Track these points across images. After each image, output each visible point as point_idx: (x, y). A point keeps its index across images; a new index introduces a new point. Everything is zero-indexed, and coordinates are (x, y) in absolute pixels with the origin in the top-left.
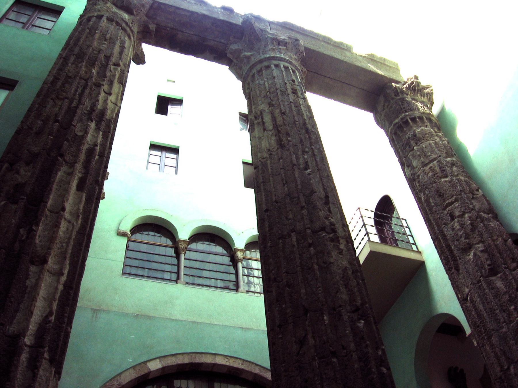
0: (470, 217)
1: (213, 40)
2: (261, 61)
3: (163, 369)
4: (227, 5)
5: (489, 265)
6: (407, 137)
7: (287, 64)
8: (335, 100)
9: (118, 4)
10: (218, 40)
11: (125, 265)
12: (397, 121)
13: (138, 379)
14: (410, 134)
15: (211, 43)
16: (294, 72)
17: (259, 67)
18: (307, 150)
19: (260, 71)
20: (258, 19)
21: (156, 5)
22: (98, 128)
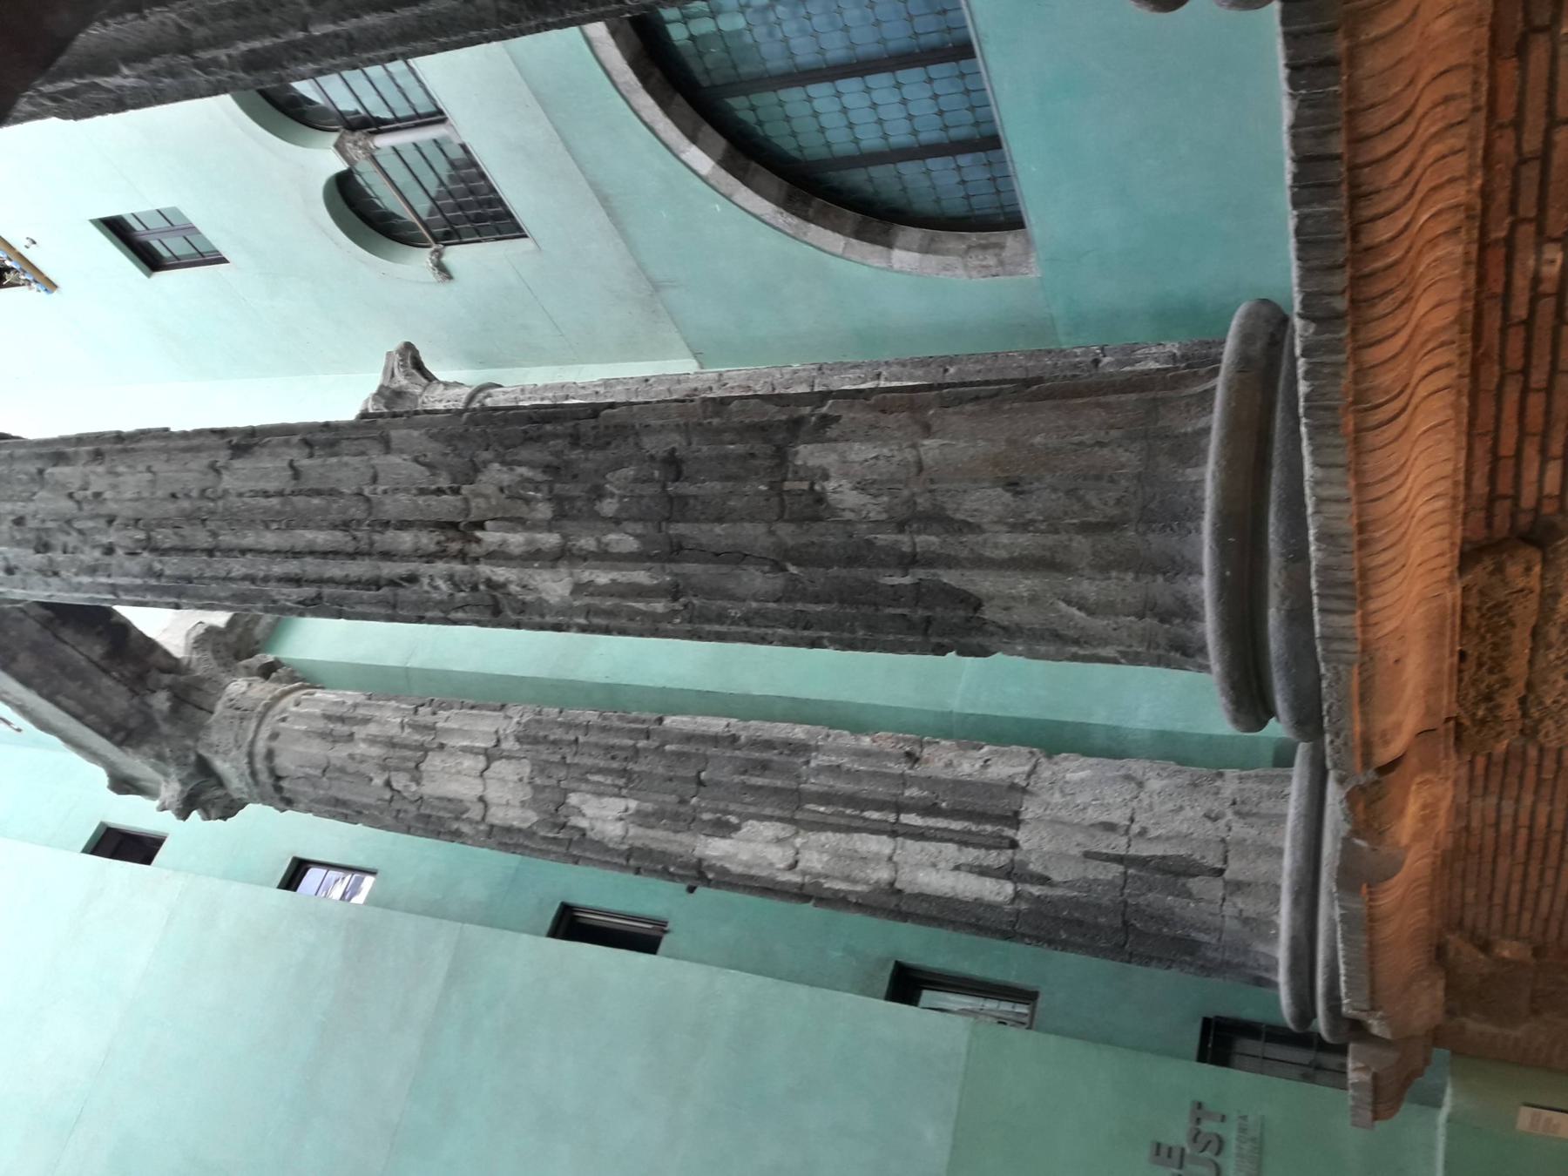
21: (120, 736)
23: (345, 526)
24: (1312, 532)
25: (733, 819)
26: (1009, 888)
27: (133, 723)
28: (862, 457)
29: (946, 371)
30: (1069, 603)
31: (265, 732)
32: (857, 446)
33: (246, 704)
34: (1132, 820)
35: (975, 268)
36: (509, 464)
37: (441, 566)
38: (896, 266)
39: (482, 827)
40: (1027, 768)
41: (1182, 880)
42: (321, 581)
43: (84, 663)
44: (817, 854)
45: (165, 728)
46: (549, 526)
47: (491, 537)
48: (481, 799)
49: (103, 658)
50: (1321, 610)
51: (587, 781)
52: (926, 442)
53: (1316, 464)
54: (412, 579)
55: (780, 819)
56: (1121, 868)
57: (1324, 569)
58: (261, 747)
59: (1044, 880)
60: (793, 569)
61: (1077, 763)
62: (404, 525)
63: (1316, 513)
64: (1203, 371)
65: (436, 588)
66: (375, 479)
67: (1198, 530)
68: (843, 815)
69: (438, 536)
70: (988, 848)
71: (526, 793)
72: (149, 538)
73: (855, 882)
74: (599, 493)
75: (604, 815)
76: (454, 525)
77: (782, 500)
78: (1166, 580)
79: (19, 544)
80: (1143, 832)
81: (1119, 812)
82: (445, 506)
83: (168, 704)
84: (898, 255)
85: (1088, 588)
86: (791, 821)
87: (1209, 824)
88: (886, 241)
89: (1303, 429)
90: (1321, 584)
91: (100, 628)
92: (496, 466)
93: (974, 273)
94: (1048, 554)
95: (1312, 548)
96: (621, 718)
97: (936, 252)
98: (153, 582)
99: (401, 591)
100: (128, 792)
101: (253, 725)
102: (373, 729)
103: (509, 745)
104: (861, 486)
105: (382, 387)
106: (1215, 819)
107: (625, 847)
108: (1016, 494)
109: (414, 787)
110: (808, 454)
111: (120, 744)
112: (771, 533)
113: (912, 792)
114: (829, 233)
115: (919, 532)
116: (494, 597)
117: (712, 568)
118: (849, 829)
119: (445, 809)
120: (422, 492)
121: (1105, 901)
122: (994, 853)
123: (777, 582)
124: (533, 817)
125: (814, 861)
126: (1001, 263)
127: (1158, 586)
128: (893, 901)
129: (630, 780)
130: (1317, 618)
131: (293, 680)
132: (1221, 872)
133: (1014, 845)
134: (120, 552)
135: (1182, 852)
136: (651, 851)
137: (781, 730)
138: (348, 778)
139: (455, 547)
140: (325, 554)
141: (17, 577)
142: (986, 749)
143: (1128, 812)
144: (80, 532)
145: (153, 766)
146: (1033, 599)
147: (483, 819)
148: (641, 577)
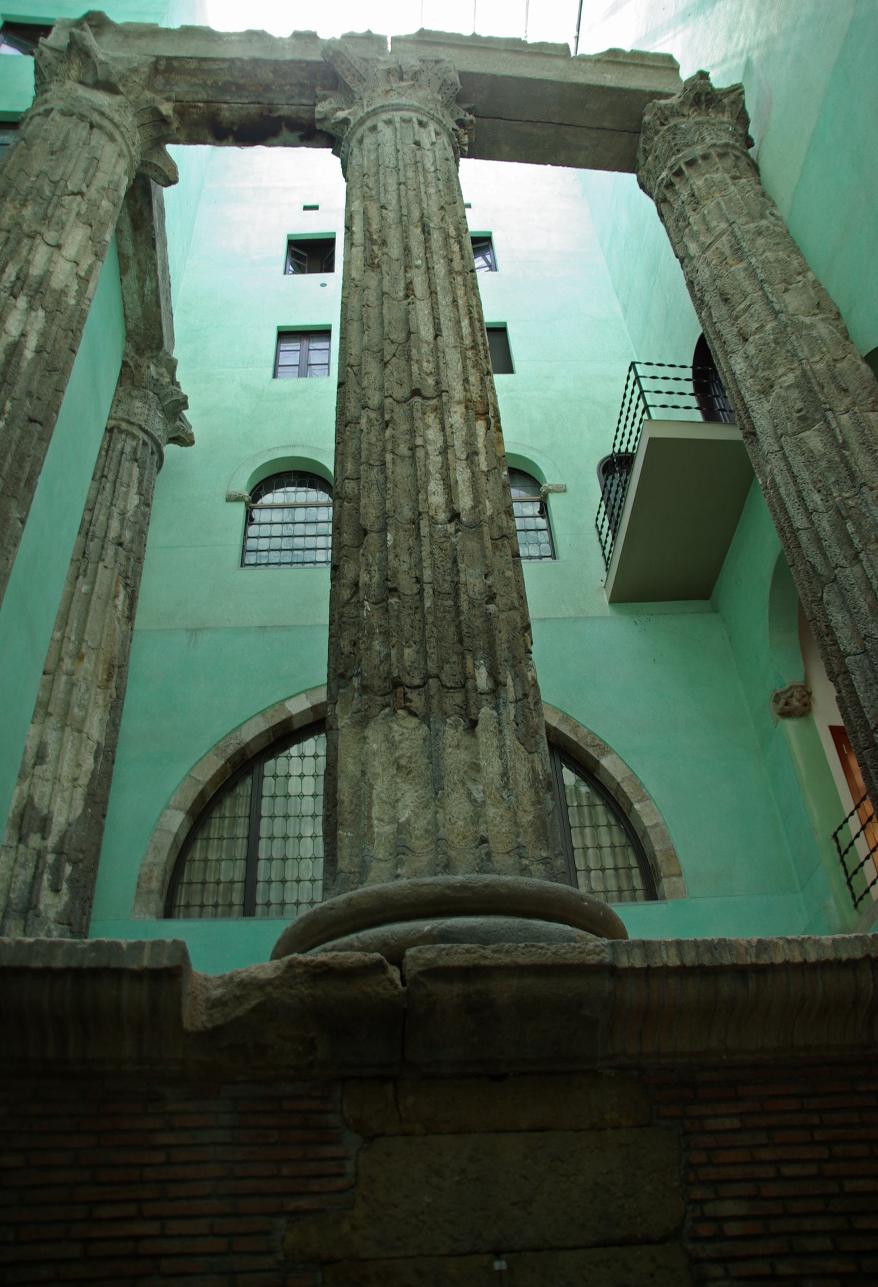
0: (773, 329)
1: (288, 104)
2: (361, 122)
4: (302, 28)
5: (800, 411)
6: (680, 203)
7: (406, 114)
8: (553, 164)
10: (295, 101)
11: (244, 551)
12: (664, 174)
13: (273, 729)
14: (685, 195)
15: (285, 111)
16: (421, 124)
17: (358, 135)
18: (419, 262)
19: (361, 141)
20: (369, 38)
21: (162, 65)
22: (31, 308)
27: (160, 80)
35: (151, 871)
38: (168, 812)
43: (228, 98)
49: (219, 109)
58: (117, 136)
83: (164, 113)
88: (190, 813)
91: (235, 128)
116: (428, 399)
124: (36, 271)
126: (150, 892)
138: (92, 171)
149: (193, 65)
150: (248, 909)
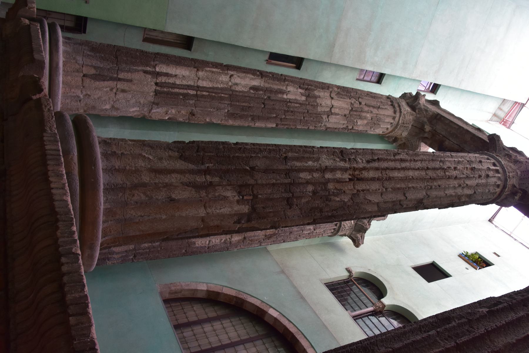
3: (276, 319)
9: (410, 104)
21: (439, 116)
23: (390, 179)
24: (65, 177)
25: (252, 91)
26: (158, 69)
28: (226, 209)
29: (186, 251)
30: (149, 158)
31: (397, 119)
32: (228, 213)
33: (402, 128)
34: (116, 94)
36: (341, 201)
37: (361, 166)
38: (205, 284)
39: (331, 89)
40: (153, 111)
41: (98, 73)
42: (395, 160)
44: (223, 80)
45: (425, 120)
46: (329, 181)
47: (346, 176)
48: (332, 98)
50: (59, 150)
51: (300, 104)
52: (203, 215)
53: (67, 201)
54: (368, 162)
55: (237, 91)
56: (119, 76)
57: (59, 165)
59: (145, 72)
60: (248, 168)
61: (135, 114)
62: (373, 179)
63: (64, 184)
64: (105, 245)
65: (361, 159)
66: (382, 195)
67: (104, 184)
68: (215, 93)
69: (362, 176)
70: (165, 83)
71: (318, 101)
72: (445, 173)
73: (210, 71)
74: (314, 193)
75: (294, 93)
76: (358, 179)
77: (252, 192)
78: (115, 167)
79: (479, 169)
80: (111, 90)
81: (120, 96)
82: (361, 186)
84: (204, 288)
85: (141, 163)
86: (233, 91)
87: (89, 93)
88: (208, 291)
89: (73, 213)
90: (60, 159)
92: (346, 200)
93: (178, 284)
94: (157, 176)
95: (64, 172)
96: (290, 125)
97: (192, 290)
98: (442, 159)
99: (371, 158)
100: (433, 101)
101: (400, 122)
102: (365, 122)
103: (324, 117)
104: (225, 198)
105: (365, 232)
106: (86, 95)
107: (287, 83)
108: (170, 197)
109: (353, 102)
110: (245, 209)
111: (438, 114)
112: (256, 180)
113: (191, 102)
114: (228, 293)
115: (204, 182)
117: (275, 167)
118: (213, 88)
119: (343, 95)
120: (368, 190)
121: (124, 66)
122: (163, 81)
123: (252, 163)
124: (316, 93)
125: (224, 78)
127: (117, 164)
128: (196, 65)
129: (286, 104)
130: (60, 148)
131: (388, 137)
132: (84, 76)
133: (156, 84)
134: (453, 168)
135: (98, 83)
136: (278, 81)
137: (237, 123)
139: (357, 173)
140: (395, 169)
141: (478, 160)
142: (167, 118)
143: (117, 97)
144: (463, 174)
145: (428, 108)
146: (161, 159)
147: (331, 92)
148: (298, 164)
149: (447, 122)
150: (177, 327)
